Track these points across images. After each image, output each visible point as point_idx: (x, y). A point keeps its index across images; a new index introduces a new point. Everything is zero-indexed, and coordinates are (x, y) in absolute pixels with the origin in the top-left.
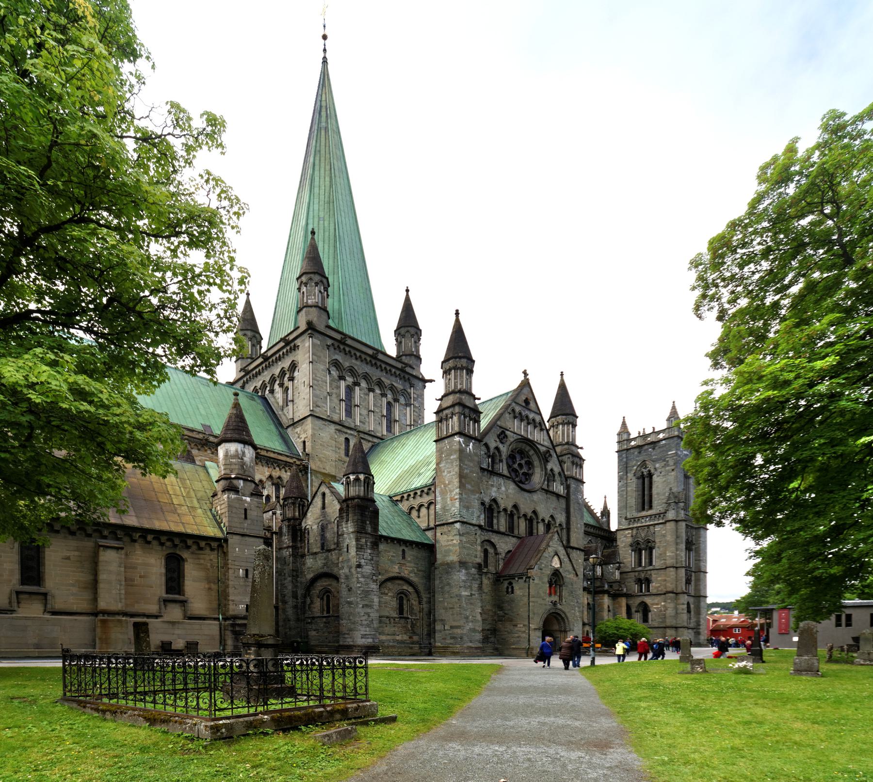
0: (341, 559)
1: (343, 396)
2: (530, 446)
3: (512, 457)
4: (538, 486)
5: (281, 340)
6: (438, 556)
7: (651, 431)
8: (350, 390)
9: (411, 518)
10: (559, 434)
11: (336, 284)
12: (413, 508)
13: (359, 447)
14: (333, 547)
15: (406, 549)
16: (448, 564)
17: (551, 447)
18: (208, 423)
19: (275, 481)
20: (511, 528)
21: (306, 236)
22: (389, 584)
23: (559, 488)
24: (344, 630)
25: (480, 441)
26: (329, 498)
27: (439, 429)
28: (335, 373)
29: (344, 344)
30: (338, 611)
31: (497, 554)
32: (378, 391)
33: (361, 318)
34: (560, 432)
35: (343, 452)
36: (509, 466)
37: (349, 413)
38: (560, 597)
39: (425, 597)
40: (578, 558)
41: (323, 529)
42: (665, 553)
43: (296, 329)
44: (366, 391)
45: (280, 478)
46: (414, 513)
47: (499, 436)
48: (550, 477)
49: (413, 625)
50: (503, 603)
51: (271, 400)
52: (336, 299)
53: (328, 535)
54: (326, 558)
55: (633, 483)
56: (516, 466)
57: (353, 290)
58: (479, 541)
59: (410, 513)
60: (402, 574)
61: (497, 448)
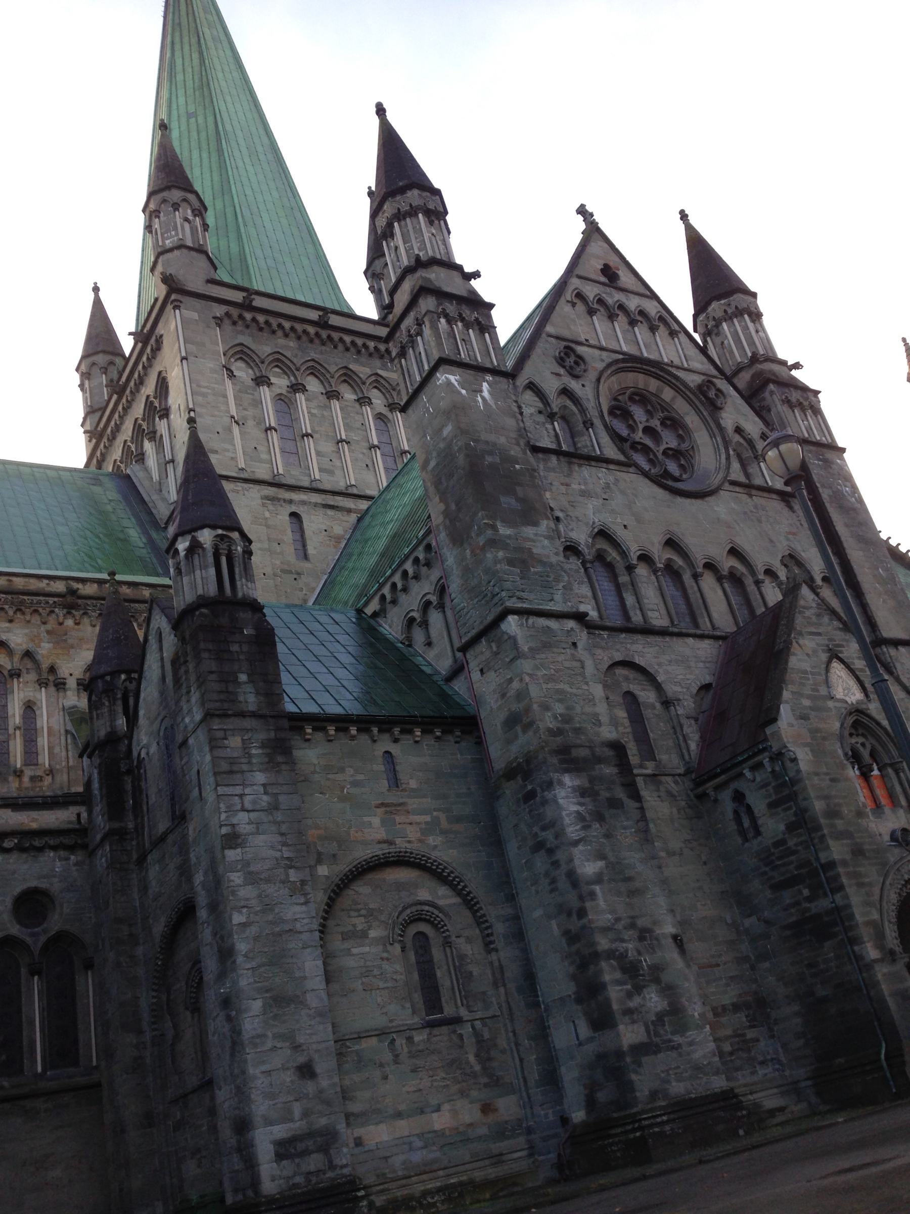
1: (271, 419)
8: (284, 402)
28: (243, 372)
32: (349, 396)
37: (294, 454)
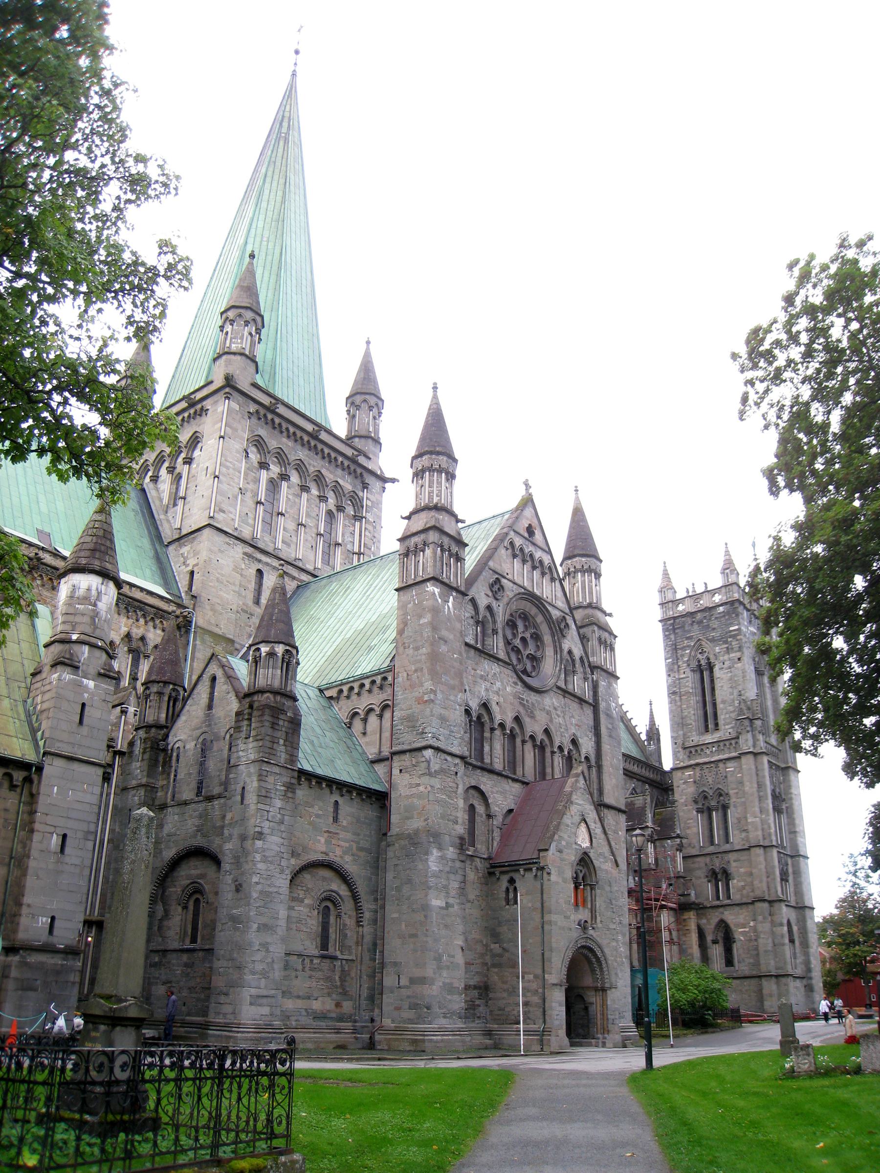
0: (229, 816)
1: (262, 496)
2: (538, 607)
3: (511, 624)
4: (551, 682)
5: (184, 398)
6: (394, 819)
7: (703, 589)
8: (273, 486)
9: (352, 735)
10: (577, 589)
11: (273, 324)
12: (356, 713)
13: (280, 591)
14: (216, 790)
15: (341, 801)
16: (409, 837)
17: (567, 611)
18: (47, 530)
19: (134, 645)
20: (512, 762)
21: (242, 258)
22: (306, 876)
23: (579, 684)
24: (218, 982)
25: (464, 594)
26: (222, 686)
27: (403, 567)
28: (254, 457)
29: (273, 412)
30: (211, 937)
31: (489, 816)
32: (315, 492)
33: (301, 375)
34: (579, 585)
35: (250, 596)
36: (508, 643)
37: (269, 525)
38: (593, 911)
39: (367, 906)
40: (618, 823)
41: (204, 749)
42: (746, 818)
43: (209, 383)
44: (298, 489)
45: (143, 639)
46: (358, 725)
47: (491, 586)
48: (569, 665)
49: (344, 975)
50: (500, 924)
51: (151, 493)
52: (271, 345)
53: (212, 765)
54: (204, 816)
55: (690, 681)
56: (517, 642)
57: (295, 336)
58: (461, 790)
59: (349, 726)
60: (332, 857)
61: (489, 608)
